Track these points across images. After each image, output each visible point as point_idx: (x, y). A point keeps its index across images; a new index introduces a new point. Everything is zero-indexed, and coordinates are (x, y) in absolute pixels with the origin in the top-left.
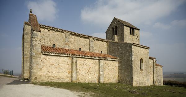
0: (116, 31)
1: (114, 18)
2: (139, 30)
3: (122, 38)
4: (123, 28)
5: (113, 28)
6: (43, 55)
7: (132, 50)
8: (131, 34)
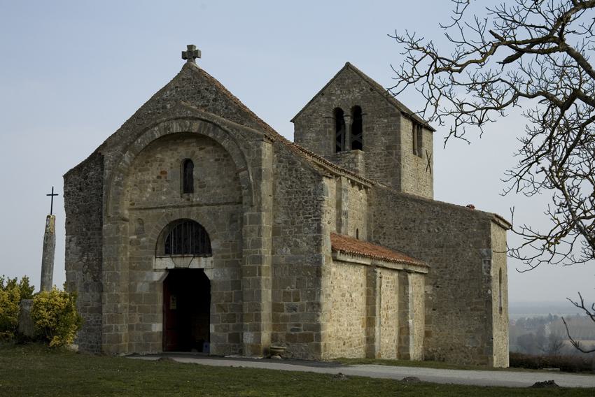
0: (357, 128)
1: (348, 65)
2: (432, 130)
3: (393, 170)
4: (399, 127)
5: (339, 113)
6: (335, 260)
7: (489, 241)
8: (415, 153)
